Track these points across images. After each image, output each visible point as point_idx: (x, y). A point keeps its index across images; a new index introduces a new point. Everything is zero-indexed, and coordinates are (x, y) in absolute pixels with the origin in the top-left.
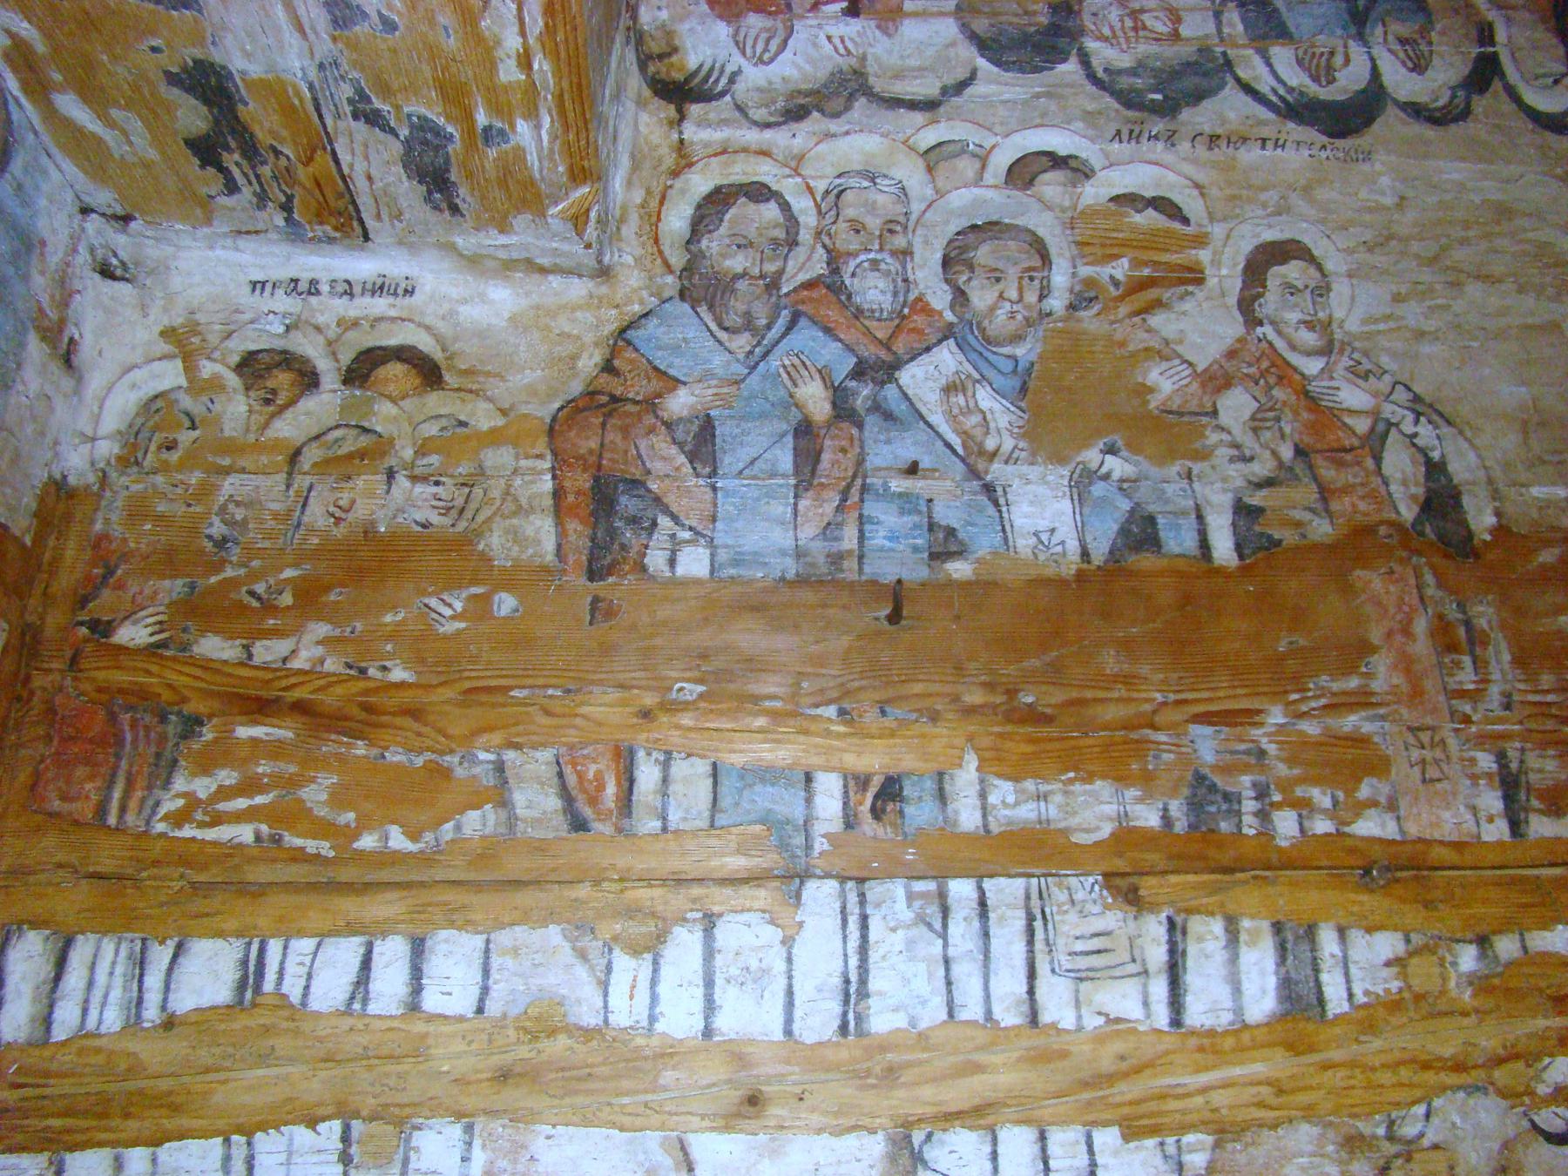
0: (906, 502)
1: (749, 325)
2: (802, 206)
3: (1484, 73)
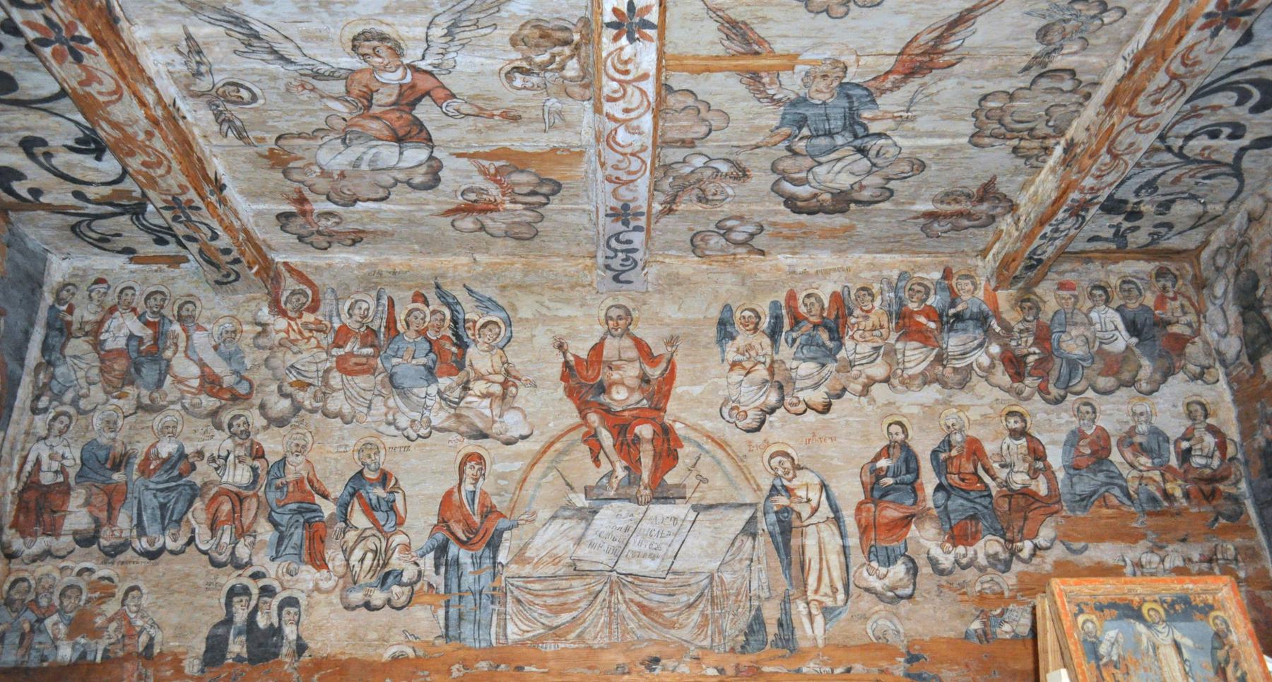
0: (38, 650)
1: (17, 611)
2: (33, 582)
3: (191, 540)
